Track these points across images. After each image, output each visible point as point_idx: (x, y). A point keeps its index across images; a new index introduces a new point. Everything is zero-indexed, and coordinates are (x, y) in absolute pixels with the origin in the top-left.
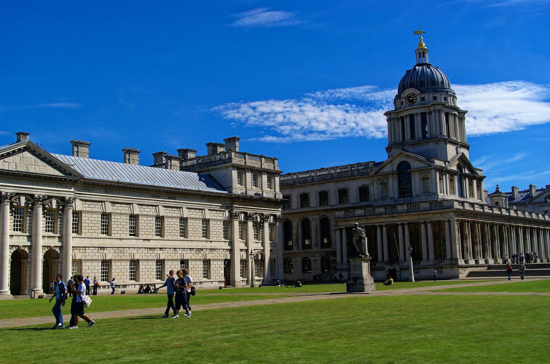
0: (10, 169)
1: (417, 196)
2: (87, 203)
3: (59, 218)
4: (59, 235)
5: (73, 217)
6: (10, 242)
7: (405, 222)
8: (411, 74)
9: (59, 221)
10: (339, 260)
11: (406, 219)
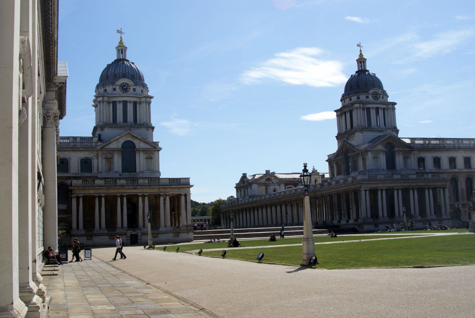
1: (142, 172)
7: (146, 194)
8: (121, 66)
10: (74, 225)
11: (147, 192)
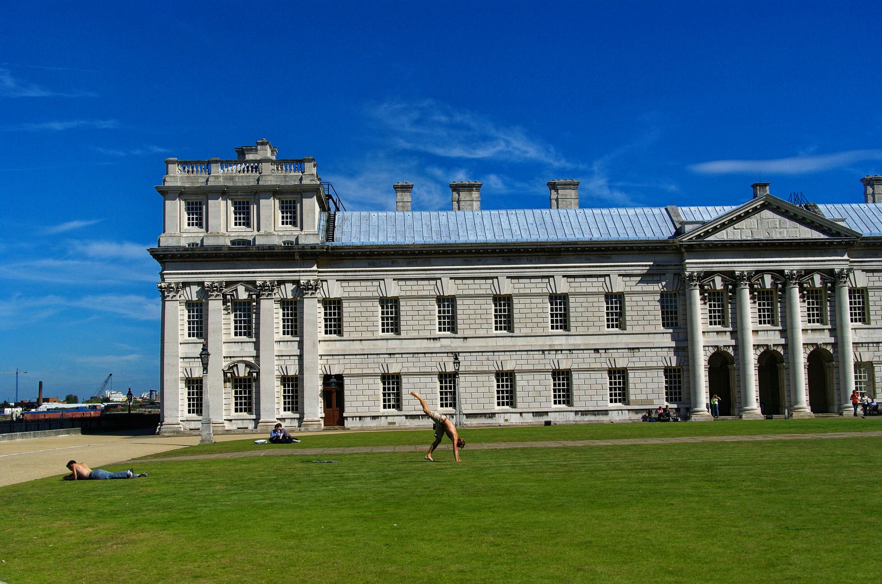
0: (744, 238)
2: (875, 274)
3: (829, 301)
4: (829, 327)
5: (850, 298)
6: (754, 341)
9: (828, 305)
